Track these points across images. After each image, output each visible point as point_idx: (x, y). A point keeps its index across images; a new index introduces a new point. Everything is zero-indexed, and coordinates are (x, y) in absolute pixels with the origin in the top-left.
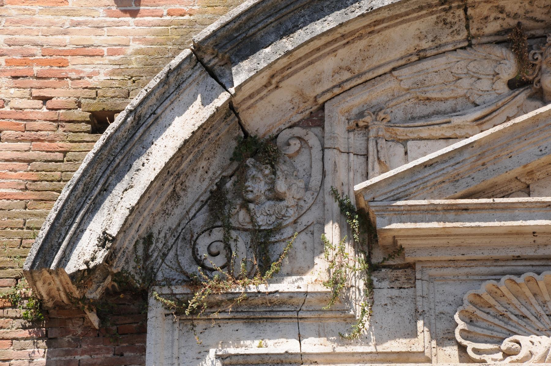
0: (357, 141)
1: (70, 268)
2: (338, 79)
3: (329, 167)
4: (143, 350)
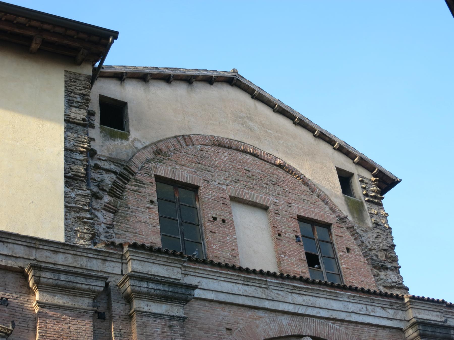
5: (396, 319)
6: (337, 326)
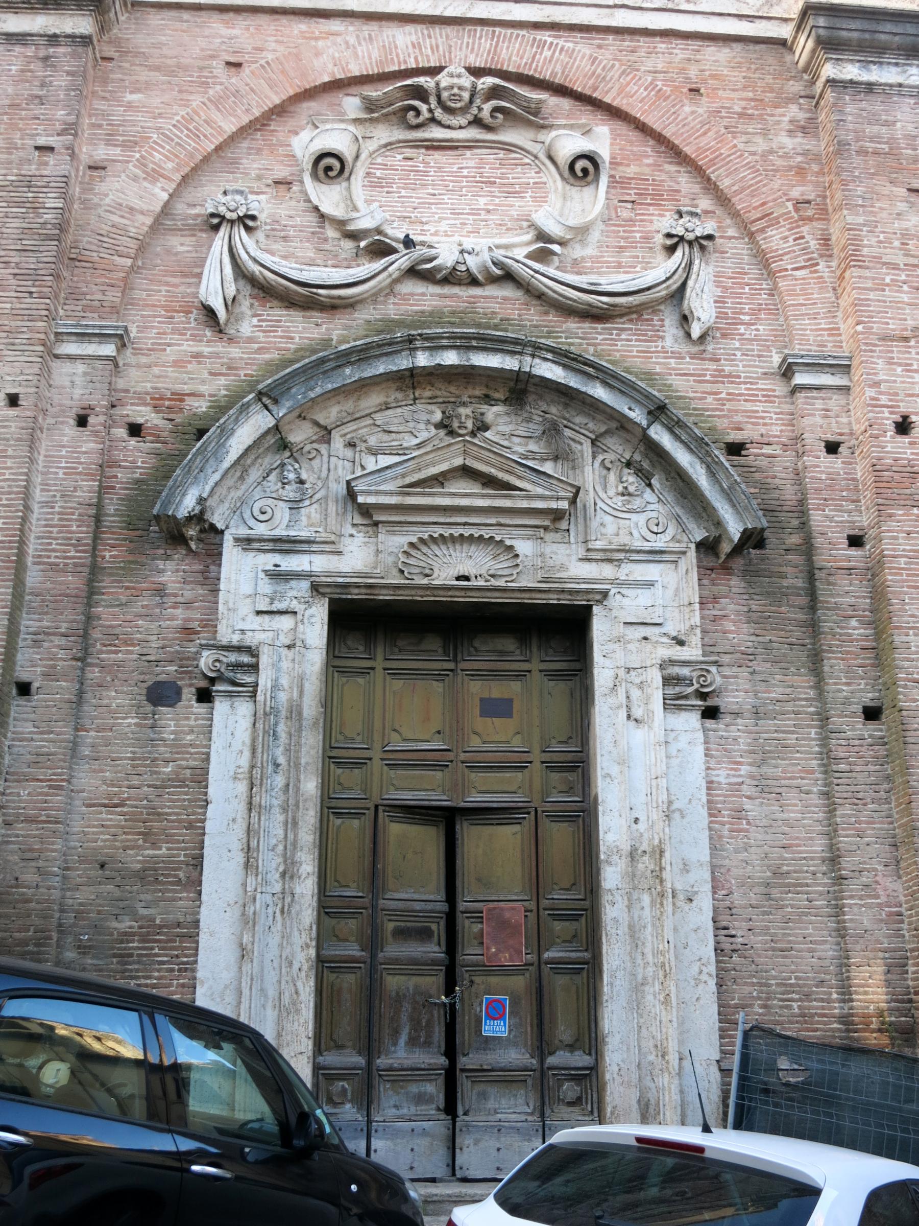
0: (349, 453)
3: (332, 466)
4: (220, 565)
5: (769, 18)
6: (566, 42)
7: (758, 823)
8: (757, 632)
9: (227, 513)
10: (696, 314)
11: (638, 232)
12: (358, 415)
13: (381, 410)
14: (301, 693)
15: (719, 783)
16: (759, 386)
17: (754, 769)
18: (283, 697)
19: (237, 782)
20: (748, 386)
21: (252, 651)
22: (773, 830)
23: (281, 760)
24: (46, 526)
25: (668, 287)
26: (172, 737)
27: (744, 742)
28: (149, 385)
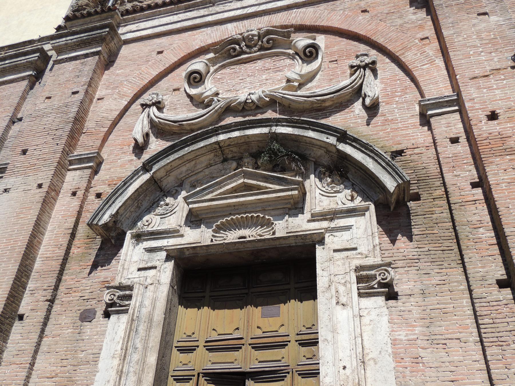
1: (100, 224)
2: (187, 173)
7: (431, 365)
8: (419, 246)
9: (130, 224)
10: (367, 94)
11: (339, 71)
12: (197, 172)
13: (207, 168)
14: (154, 308)
15: (401, 340)
16: (409, 122)
17: (425, 329)
18: (144, 311)
19: (114, 359)
20: (403, 123)
21: (130, 288)
22: (442, 369)
23: (139, 345)
24: (49, 240)
25: (352, 87)
26: (87, 337)
27: (416, 313)
28: (108, 176)
